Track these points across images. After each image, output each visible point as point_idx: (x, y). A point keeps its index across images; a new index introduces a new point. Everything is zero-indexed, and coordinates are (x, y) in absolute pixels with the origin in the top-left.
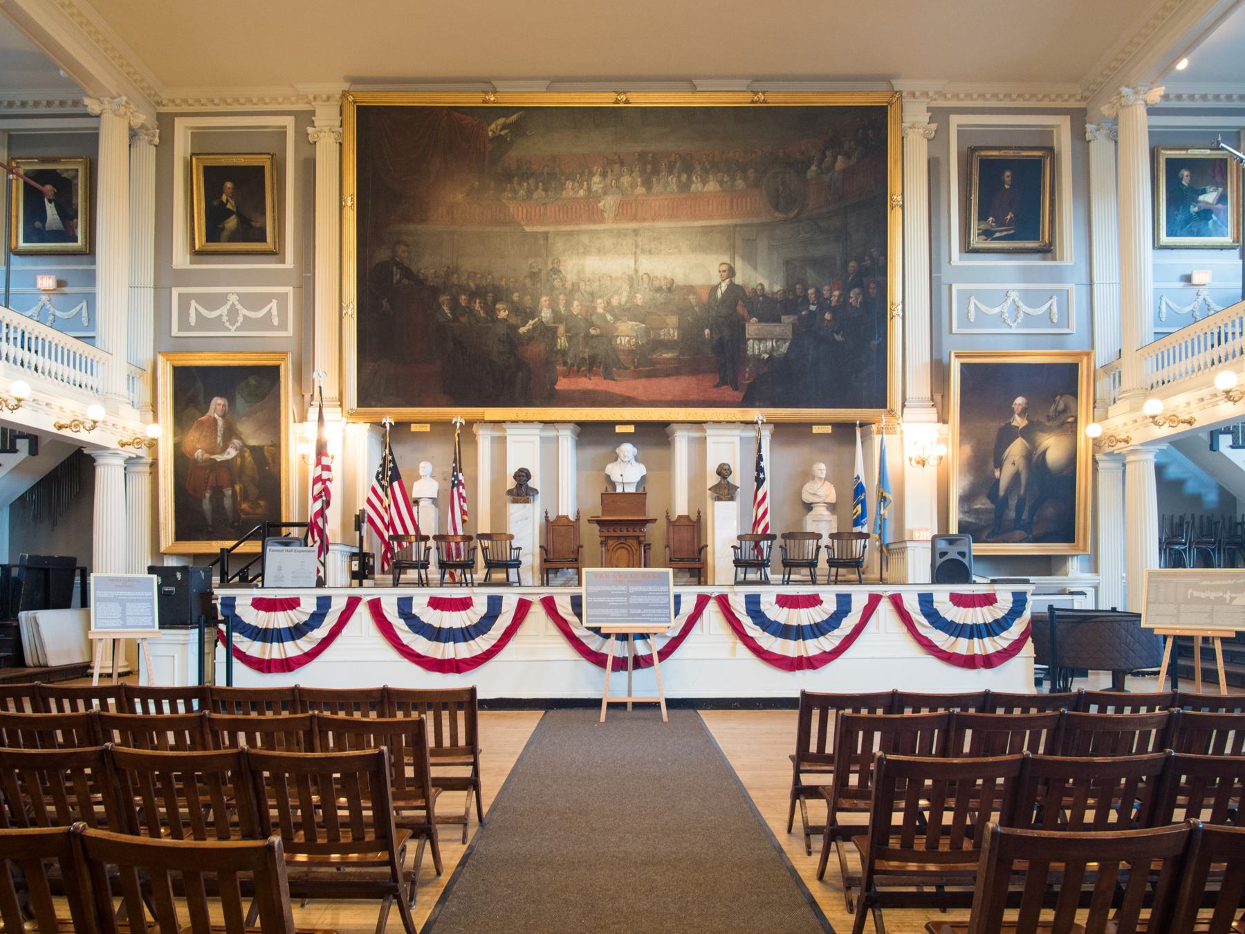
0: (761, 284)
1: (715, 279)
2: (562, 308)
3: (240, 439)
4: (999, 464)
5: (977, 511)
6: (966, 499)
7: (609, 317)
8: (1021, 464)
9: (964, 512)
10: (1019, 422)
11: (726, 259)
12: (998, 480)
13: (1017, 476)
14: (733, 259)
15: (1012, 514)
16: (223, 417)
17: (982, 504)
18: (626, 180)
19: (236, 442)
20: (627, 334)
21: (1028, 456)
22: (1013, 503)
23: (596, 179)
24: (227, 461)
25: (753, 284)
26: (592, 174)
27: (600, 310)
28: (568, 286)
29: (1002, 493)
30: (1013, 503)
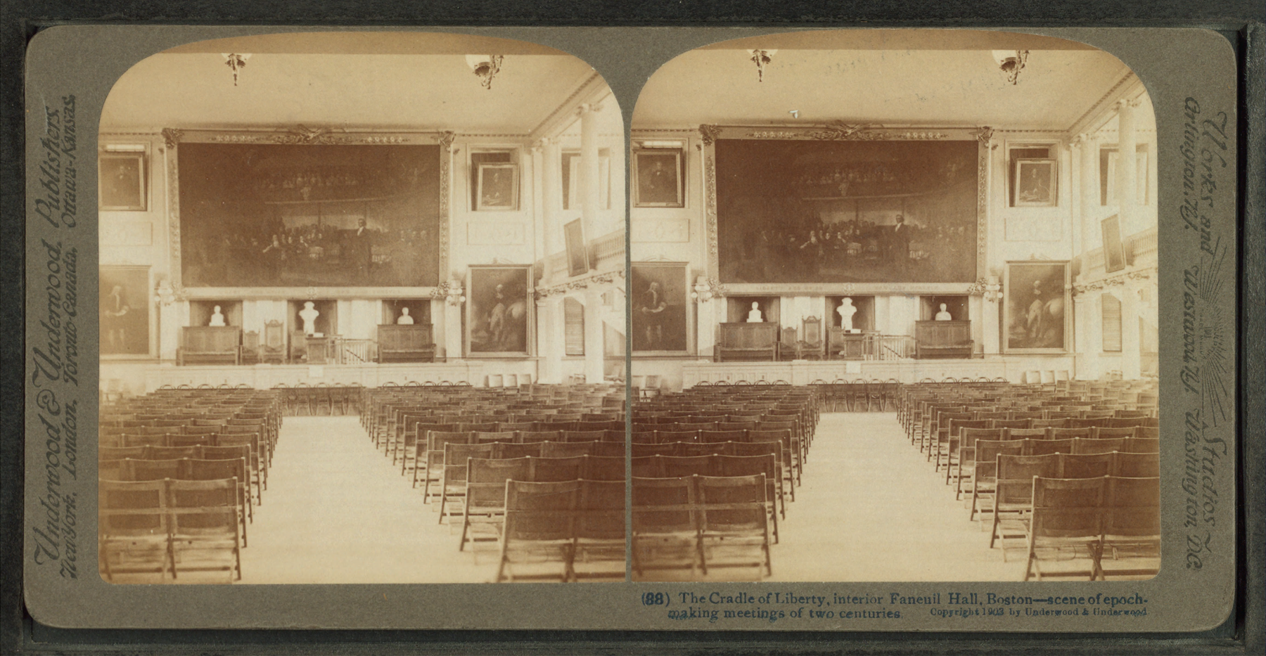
0: (379, 229)
1: (357, 227)
2: (284, 241)
3: (128, 305)
4: (490, 315)
5: (480, 338)
6: (475, 331)
7: (306, 245)
8: (501, 316)
9: (473, 338)
10: (500, 296)
11: (362, 217)
12: (489, 324)
13: (499, 319)
14: (365, 216)
15: (496, 339)
16: (120, 295)
17: (483, 333)
18: (313, 180)
19: (126, 307)
20: (315, 251)
21: (504, 312)
22: (497, 333)
23: (300, 179)
24: (121, 317)
25: (375, 229)
26: (297, 177)
27: (302, 241)
28: (286, 228)
29: (491, 329)
30: (497, 333)
